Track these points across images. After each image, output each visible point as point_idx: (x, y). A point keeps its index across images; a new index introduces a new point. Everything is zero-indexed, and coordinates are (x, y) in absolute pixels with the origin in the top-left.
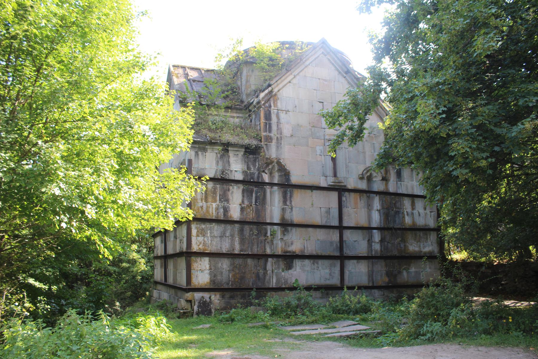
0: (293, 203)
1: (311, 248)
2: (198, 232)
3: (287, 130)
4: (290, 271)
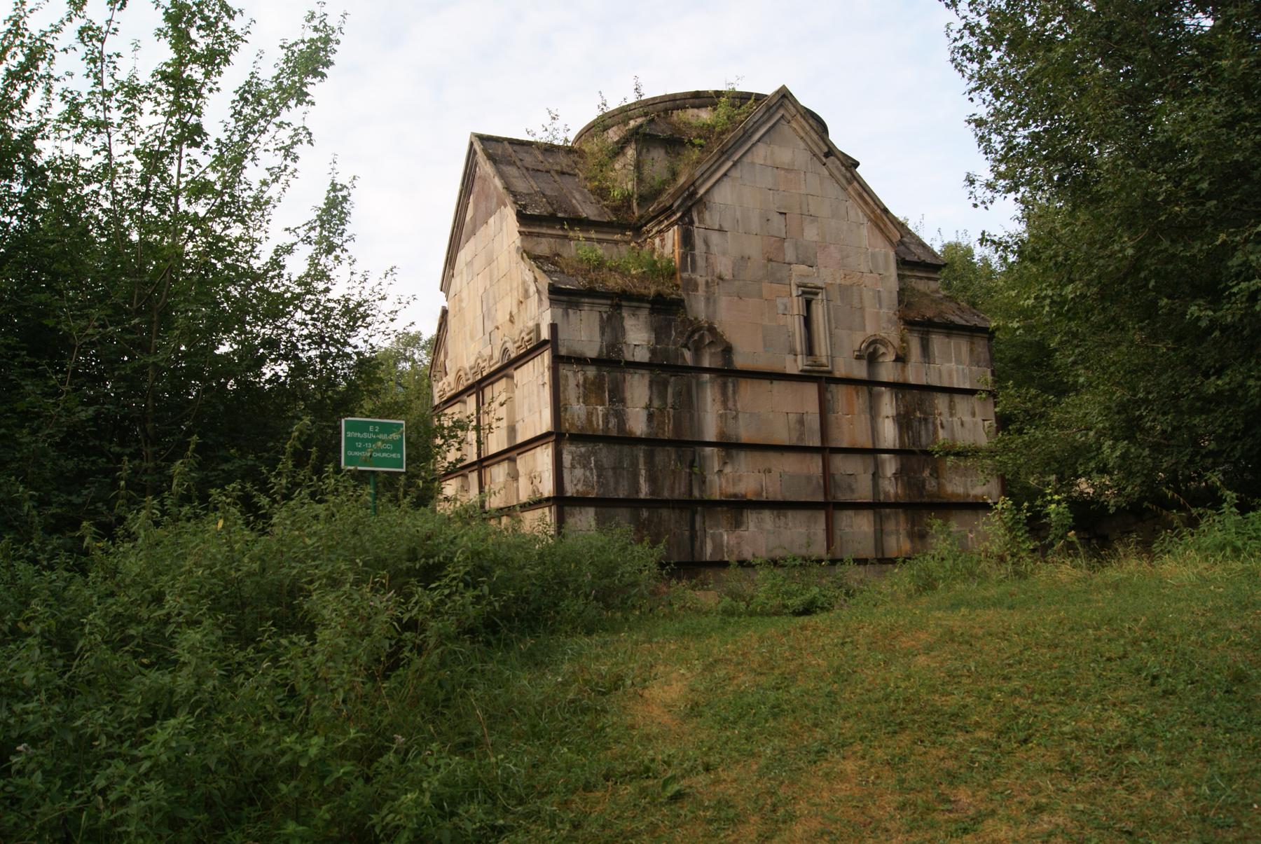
0: (739, 406)
1: (774, 490)
2: (573, 459)
3: (723, 266)
4: (739, 532)
